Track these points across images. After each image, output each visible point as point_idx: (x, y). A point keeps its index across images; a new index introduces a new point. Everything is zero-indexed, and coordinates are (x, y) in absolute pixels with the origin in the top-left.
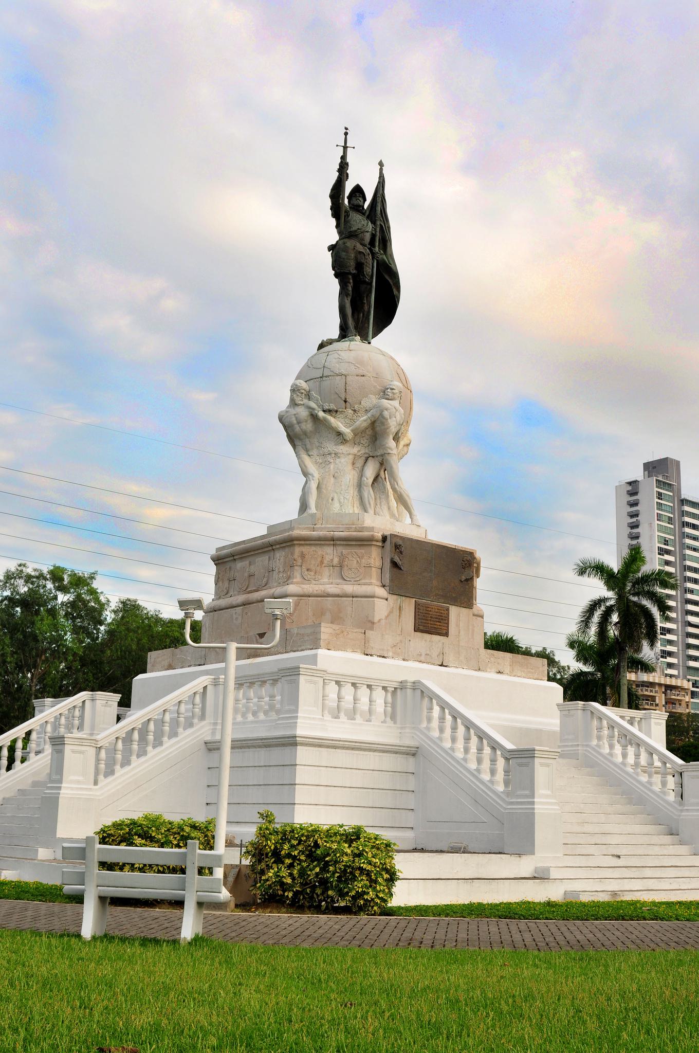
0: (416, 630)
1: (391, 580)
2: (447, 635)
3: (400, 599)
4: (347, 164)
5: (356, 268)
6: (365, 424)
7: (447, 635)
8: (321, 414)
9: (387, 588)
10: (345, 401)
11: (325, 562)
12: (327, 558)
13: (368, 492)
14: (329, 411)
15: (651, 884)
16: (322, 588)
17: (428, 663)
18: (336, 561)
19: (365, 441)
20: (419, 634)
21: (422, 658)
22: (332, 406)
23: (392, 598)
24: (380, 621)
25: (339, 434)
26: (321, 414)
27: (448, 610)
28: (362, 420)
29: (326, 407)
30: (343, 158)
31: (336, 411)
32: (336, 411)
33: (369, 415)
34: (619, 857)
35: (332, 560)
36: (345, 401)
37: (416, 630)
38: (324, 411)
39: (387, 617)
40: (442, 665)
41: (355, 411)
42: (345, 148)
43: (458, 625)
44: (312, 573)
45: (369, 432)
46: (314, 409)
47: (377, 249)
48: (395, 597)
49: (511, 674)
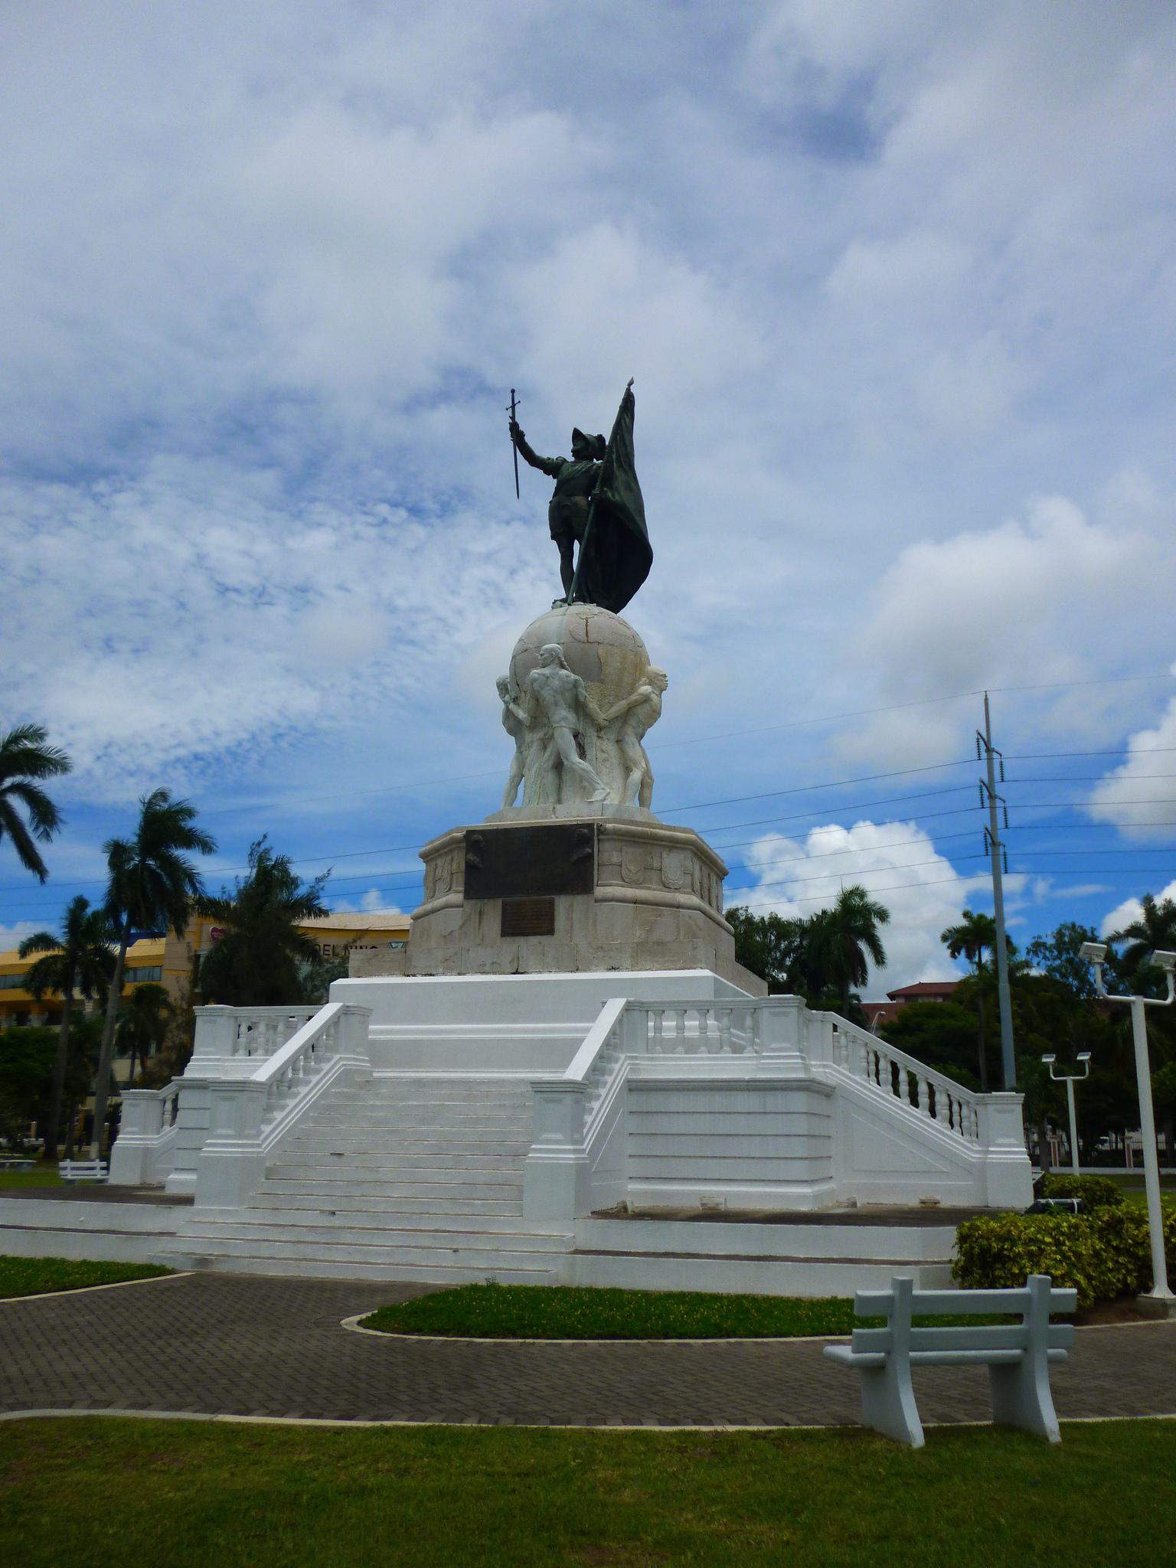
0: (504, 934)
2: (550, 931)
3: (479, 903)
7: (550, 931)
8: (512, 706)
13: (550, 778)
15: (309, 1251)
17: (494, 973)
20: (509, 939)
21: (487, 968)
23: (469, 905)
24: (451, 933)
27: (552, 903)
30: (513, 418)
34: (333, 1213)
37: (504, 934)
39: (461, 928)
40: (516, 973)
43: (569, 918)
47: (596, 491)
48: (473, 902)
49: (633, 969)
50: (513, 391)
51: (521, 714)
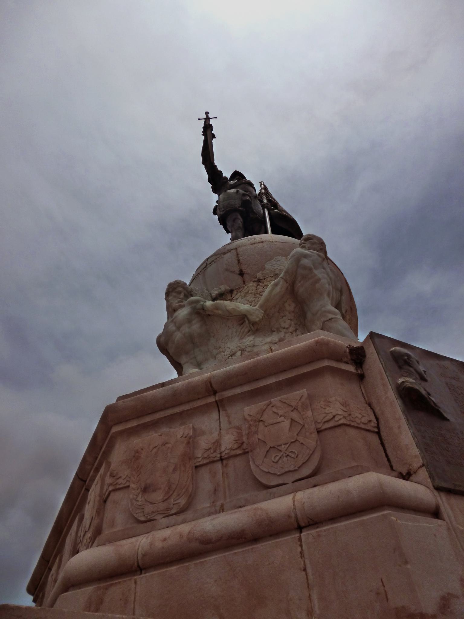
1: (425, 447)
4: (211, 125)
5: (241, 206)
6: (278, 289)
9: (423, 474)
10: (241, 274)
11: (199, 453)
12: (204, 443)
14: (221, 296)
16: (185, 528)
18: (228, 441)
19: (286, 322)
22: (223, 288)
25: (242, 318)
26: (209, 303)
28: (271, 289)
29: (215, 292)
31: (231, 292)
32: (231, 292)
33: (282, 275)
35: (217, 443)
36: (241, 274)
38: (214, 300)
41: (259, 281)
42: (207, 119)
44: (158, 496)
45: (290, 306)
46: (197, 302)
50: (207, 113)
51: (240, 305)
